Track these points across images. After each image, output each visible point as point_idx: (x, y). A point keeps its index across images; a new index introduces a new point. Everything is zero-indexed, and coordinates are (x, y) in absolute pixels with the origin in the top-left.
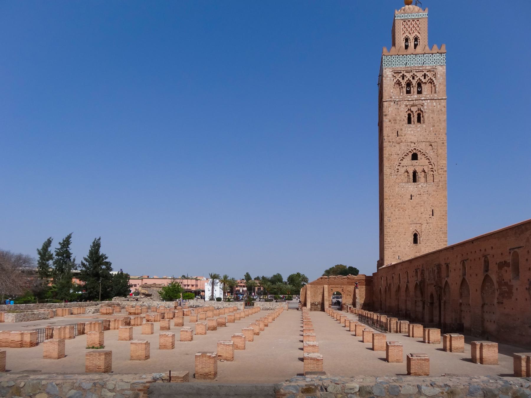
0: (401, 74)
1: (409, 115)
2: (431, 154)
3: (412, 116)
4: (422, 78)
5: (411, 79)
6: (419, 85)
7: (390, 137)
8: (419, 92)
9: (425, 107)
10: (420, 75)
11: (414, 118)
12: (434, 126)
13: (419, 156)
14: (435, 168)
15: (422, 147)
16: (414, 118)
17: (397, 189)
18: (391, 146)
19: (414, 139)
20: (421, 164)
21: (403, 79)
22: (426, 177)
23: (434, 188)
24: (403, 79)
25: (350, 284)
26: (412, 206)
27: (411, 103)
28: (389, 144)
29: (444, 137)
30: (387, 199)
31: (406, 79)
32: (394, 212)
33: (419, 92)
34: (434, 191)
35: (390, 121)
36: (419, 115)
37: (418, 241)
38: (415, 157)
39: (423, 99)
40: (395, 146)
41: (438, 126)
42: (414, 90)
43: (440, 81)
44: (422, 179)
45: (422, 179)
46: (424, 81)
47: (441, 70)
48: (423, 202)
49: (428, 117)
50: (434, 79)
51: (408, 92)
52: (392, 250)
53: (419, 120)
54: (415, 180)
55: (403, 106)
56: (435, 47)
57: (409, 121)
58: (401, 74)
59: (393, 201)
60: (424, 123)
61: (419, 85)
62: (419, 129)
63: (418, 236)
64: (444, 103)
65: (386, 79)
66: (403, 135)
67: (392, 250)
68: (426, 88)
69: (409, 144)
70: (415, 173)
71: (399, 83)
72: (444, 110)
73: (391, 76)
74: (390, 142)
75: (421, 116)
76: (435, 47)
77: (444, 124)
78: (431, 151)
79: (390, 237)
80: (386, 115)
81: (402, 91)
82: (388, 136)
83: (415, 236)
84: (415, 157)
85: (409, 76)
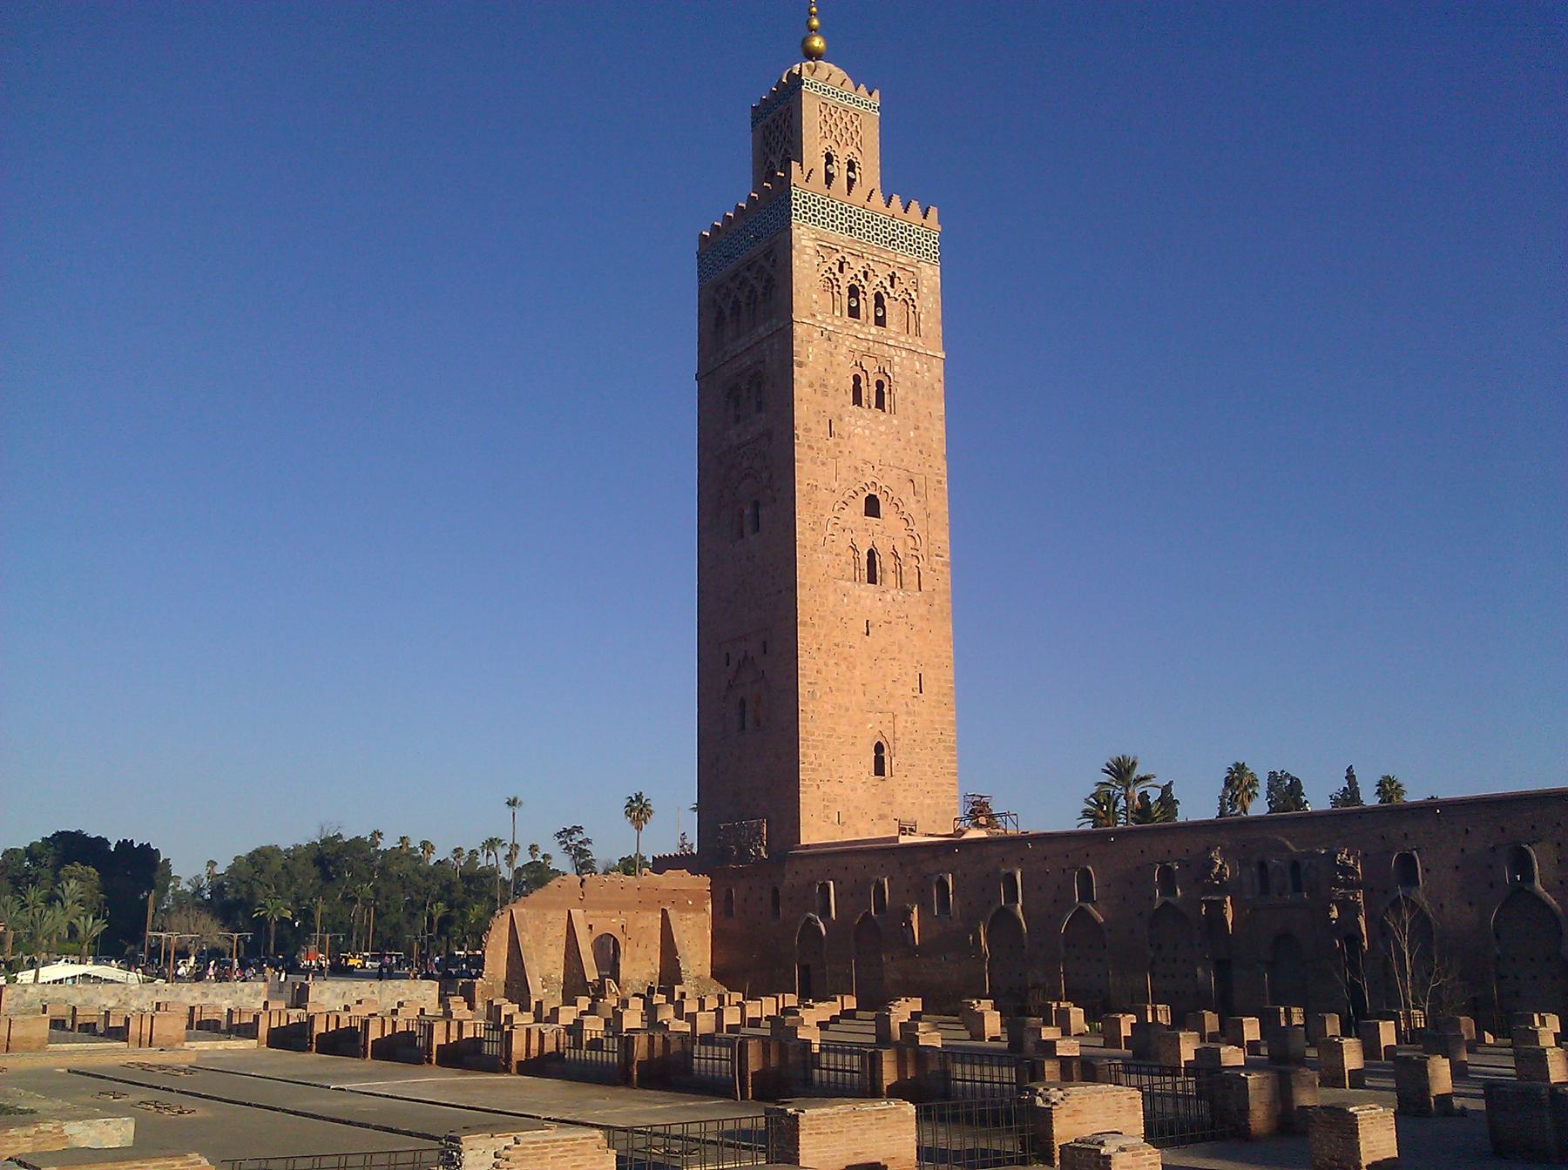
0: (838, 256)
1: (857, 379)
2: (911, 506)
3: (863, 384)
4: (887, 284)
5: (861, 277)
6: (878, 297)
7: (812, 434)
8: (880, 322)
9: (896, 369)
10: (882, 275)
11: (870, 393)
12: (917, 428)
13: (883, 508)
14: (923, 550)
15: (889, 483)
16: (870, 393)
17: (831, 598)
18: (813, 461)
19: (872, 454)
20: (886, 533)
21: (841, 270)
22: (899, 574)
23: (923, 609)
24: (841, 270)
25: (643, 905)
26: (870, 657)
27: (863, 346)
28: (810, 453)
29: (941, 466)
30: (805, 624)
31: (849, 274)
32: (824, 668)
33: (880, 322)
34: (921, 617)
35: (811, 386)
36: (880, 384)
37: (887, 768)
38: (872, 507)
39: (891, 342)
40: (823, 464)
41: (927, 429)
42: (867, 307)
43: (930, 304)
44: (891, 579)
45: (891, 579)
46: (889, 289)
47: (931, 274)
48: (895, 648)
49: (904, 399)
50: (914, 295)
51: (854, 313)
52: (820, 793)
53: (880, 404)
54: (872, 579)
55: (844, 350)
56: (915, 206)
57: (857, 400)
58: (838, 256)
59: (823, 633)
60: (893, 412)
61: (879, 299)
62: (882, 428)
63: (886, 750)
64: (938, 370)
65: (799, 257)
66: (845, 435)
67: (820, 793)
68: (893, 310)
69: (860, 464)
70: (871, 554)
71: (832, 283)
72: (939, 388)
73: (812, 252)
74: (810, 447)
75: (886, 390)
76: (915, 206)
77: (940, 428)
78: (913, 499)
79: (815, 747)
80: (801, 365)
81: (837, 304)
82: (808, 430)
83: (879, 748)
84: (872, 507)
85: (858, 266)
